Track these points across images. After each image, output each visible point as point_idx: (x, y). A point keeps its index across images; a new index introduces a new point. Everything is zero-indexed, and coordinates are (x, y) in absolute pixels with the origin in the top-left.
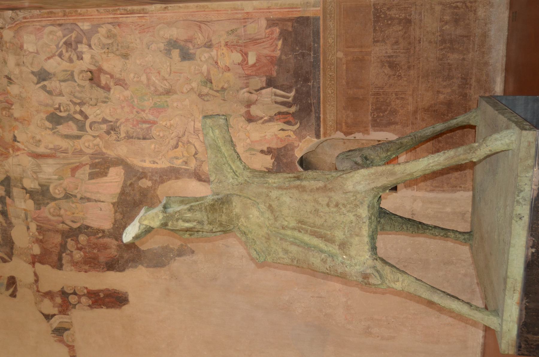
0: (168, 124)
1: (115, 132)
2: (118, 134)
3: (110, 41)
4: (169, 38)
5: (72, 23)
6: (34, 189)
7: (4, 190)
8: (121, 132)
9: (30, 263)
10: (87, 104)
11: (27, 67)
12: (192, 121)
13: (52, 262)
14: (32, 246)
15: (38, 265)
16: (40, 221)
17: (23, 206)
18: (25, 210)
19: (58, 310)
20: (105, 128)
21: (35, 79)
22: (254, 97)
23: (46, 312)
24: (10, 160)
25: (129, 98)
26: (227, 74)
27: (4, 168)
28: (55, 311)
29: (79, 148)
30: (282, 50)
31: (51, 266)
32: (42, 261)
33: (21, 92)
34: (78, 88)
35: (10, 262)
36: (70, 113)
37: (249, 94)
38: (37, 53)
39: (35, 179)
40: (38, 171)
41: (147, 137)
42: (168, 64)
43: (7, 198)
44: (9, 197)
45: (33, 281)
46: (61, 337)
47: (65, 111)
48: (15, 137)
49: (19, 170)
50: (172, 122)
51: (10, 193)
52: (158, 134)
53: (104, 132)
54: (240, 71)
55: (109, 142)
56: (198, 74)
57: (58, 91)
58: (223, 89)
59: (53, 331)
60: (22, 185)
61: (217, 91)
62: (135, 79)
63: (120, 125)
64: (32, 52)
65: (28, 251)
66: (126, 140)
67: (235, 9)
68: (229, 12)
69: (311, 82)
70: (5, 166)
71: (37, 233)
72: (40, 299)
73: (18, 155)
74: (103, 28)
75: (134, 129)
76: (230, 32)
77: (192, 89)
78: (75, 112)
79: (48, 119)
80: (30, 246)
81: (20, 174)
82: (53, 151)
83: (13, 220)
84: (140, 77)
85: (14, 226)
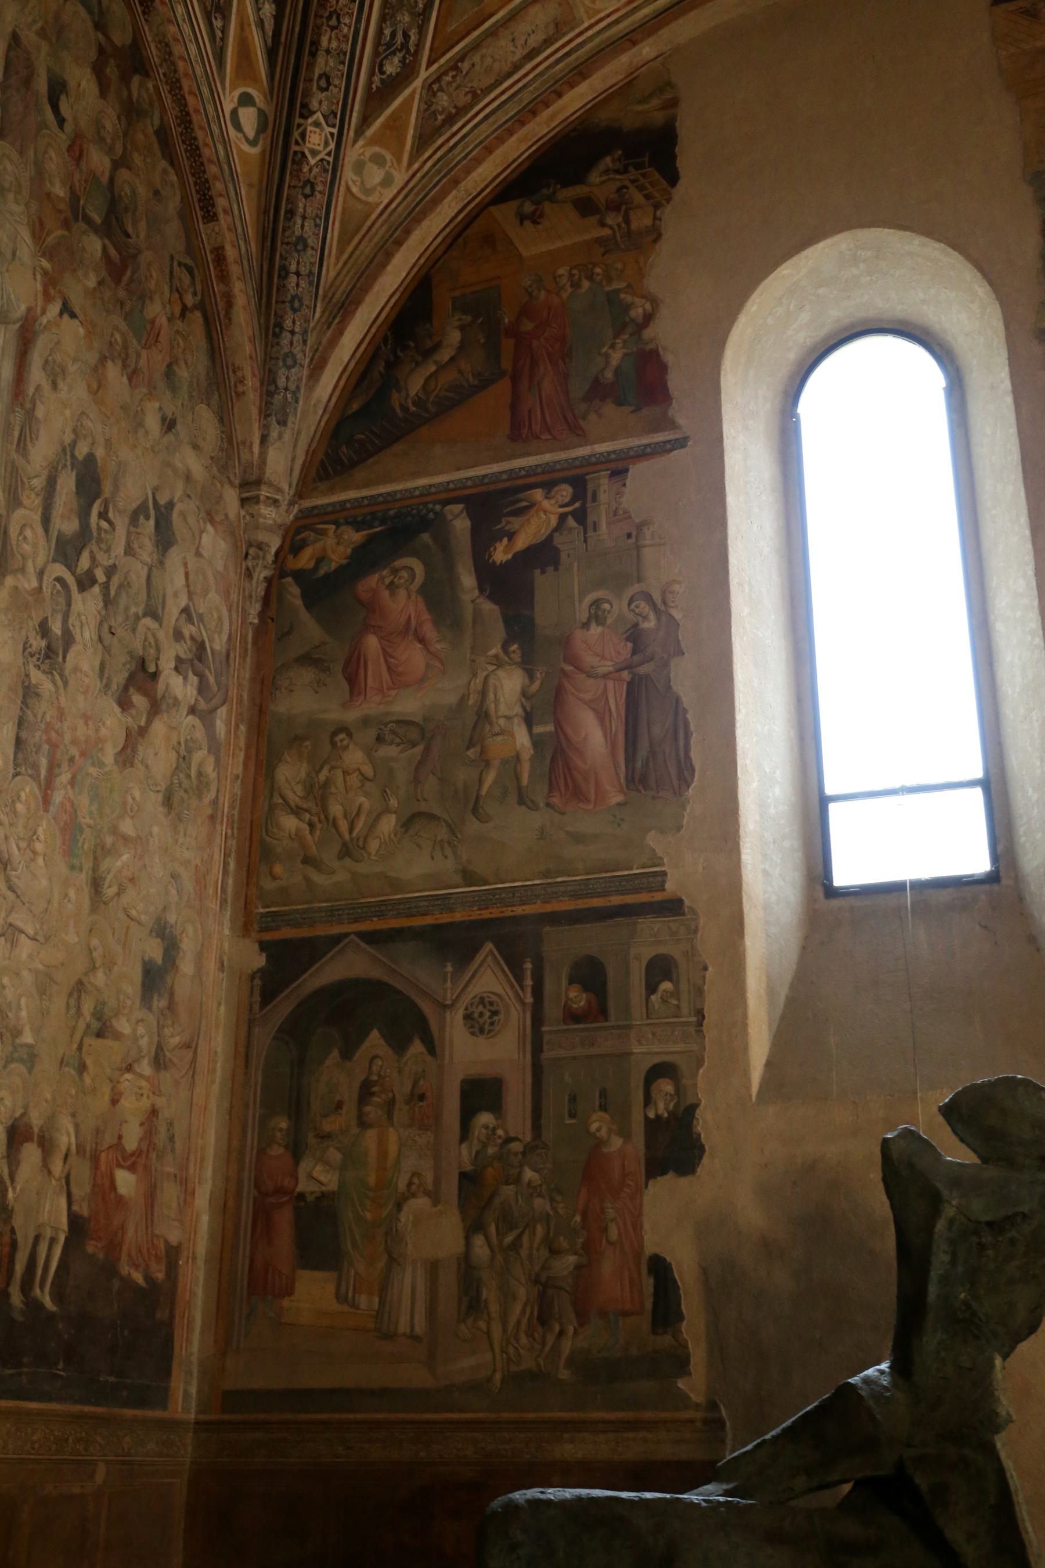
0: (39, 847)
1: (43, 652)
2: (39, 658)
3: (193, 773)
4: (181, 946)
5: (227, 690)
8: (43, 677)
10: (104, 612)
11: (181, 500)
12: (36, 934)
20: (53, 628)
21: (162, 501)
22: (57, 1167)
24: (25, 234)
25: (100, 755)
26: (106, 1090)
29: (26, 502)
30: (128, 1283)
34: (133, 610)
36: (93, 542)
37: (64, 1150)
38: (198, 554)
41: (20, 756)
42: (143, 918)
47: (99, 528)
48: (73, 316)
50: (40, 860)
52: (23, 795)
53: (47, 618)
54: (109, 1139)
55: (26, 616)
56: (118, 999)
57: (136, 546)
58: (82, 1068)
61: (80, 1048)
62: (129, 799)
63: (54, 683)
64: (200, 538)
66: (23, 674)
67: (203, 1160)
68: (200, 1141)
69: (63, 1370)
74: (214, 771)
75: (42, 721)
76: (171, 1131)
77: (94, 968)
78: (93, 558)
79: (90, 458)
82: (28, 406)
84: (132, 817)
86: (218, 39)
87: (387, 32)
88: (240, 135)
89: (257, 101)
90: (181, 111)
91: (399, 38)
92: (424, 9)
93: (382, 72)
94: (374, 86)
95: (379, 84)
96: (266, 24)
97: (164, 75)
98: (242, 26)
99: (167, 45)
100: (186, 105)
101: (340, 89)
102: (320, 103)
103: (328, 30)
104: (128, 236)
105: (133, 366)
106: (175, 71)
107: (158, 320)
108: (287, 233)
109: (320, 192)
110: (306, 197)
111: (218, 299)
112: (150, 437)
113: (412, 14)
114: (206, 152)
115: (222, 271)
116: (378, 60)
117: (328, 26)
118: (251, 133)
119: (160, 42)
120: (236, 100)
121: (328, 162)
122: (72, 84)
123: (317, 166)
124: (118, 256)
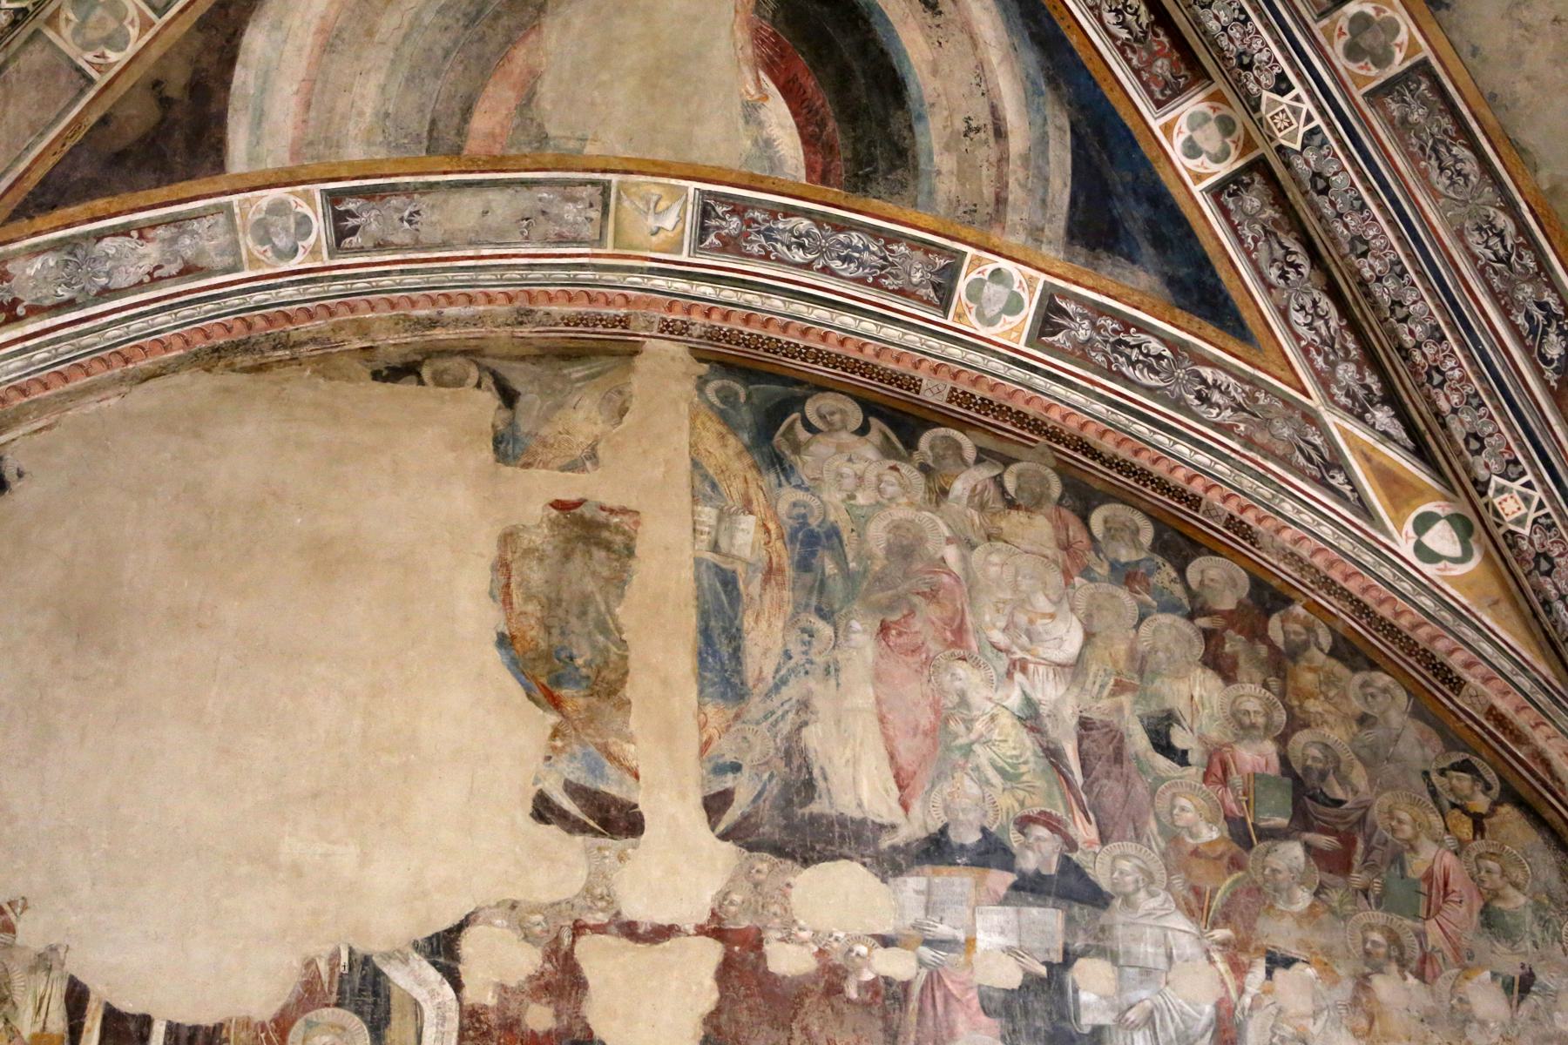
6: (1076, 1001)
7: (1044, 872)
9: (720, 920)
13: (737, 1022)
14: (803, 943)
15: (713, 952)
16: (929, 1001)
17: (984, 940)
18: (971, 942)
19: (486, 1007)
23: (468, 945)
24: (1179, 922)
27: (1138, 890)
28: (481, 990)
31: (718, 1011)
32: (733, 973)
33: (1483, 1024)
35: (713, 830)
39: (1122, 1013)
40: (1160, 1035)
43: (1011, 878)
44: (1015, 887)
45: (628, 914)
46: (334, 998)
48: (1288, 963)
49: (1148, 951)
51: (1032, 891)
59: (367, 960)
60: (1084, 953)
65: (777, 920)
70: (1152, 895)
71: (868, 976)
72: (538, 929)
73: (1211, 961)
80: (805, 935)
81: (1128, 953)
83: (913, 883)
85: (884, 881)
86: (1349, 494)
87: (1521, 320)
88: (1441, 565)
89: (1438, 511)
90: (1351, 603)
91: (1538, 315)
92: (1539, 264)
93: (1549, 362)
94: (1553, 383)
95: (1556, 377)
96: (1392, 431)
97: (1312, 582)
98: (1366, 457)
99: (1292, 554)
100: (1350, 595)
101: (1500, 431)
102: (1487, 466)
103: (1438, 390)
104: (1339, 803)
105: (1418, 954)
106: (1317, 571)
107: (1436, 867)
108: (1560, 628)
109: (1561, 555)
110: (1548, 573)
111: (1532, 765)
112: (1492, 1025)
113: (1529, 281)
114: (1404, 622)
115: (1511, 732)
116: (1536, 355)
117: (1435, 387)
118: (1455, 550)
119: (1285, 557)
120: (1412, 533)
121: (1547, 516)
122: (1180, 705)
123: (1533, 531)
124: (1332, 839)
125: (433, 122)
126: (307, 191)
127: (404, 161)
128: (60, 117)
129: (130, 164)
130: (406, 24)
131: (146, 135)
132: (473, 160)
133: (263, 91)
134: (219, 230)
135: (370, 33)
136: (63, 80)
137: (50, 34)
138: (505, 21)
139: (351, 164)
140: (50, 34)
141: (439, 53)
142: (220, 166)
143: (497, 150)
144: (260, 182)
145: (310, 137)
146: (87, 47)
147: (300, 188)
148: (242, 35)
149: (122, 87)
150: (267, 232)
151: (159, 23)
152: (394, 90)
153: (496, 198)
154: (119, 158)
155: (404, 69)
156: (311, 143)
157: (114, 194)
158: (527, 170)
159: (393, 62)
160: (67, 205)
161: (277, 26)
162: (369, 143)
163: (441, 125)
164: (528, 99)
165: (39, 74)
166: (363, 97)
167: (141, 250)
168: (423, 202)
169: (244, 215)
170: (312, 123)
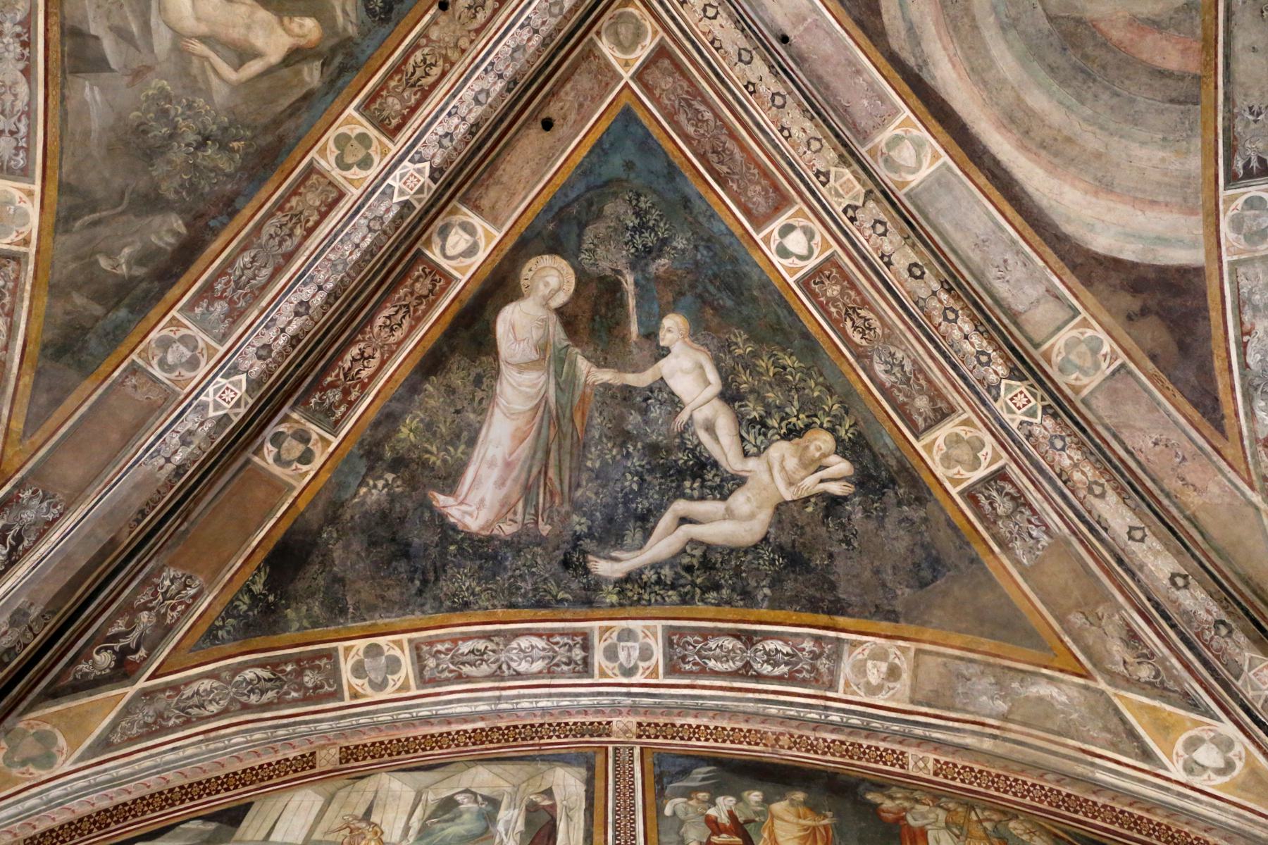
125: (1172, 101)
126: (1225, 201)
127: (1204, 123)
128: (1146, 390)
129: (1188, 340)
130: (1090, 128)
131: (1169, 327)
132: (1205, 65)
133: (1140, 237)
134: (1251, 272)
135: (1098, 156)
136: (1119, 385)
137: (1085, 392)
138: (1089, 50)
139: (1204, 167)
140: (1085, 392)
141: (1115, 101)
142: (1198, 271)
143: (1198, 46)
144: (1213, 240)
145: (1179, 200)
146: (1097, 367)
147: (1221, 207)
148: (1097, 253)
149: (1129, 342)
150: (1256, 233)
151: (1084, 314)
152: (1144, 135)
153: (1239, 44)
154: (1183, 348)
155: (1127, 128)
156: (1185, 199)
157: (1211, 353)
158: (1216, 18)
159: (1121, 137)
160: (1216, 389)
161: (1091, 228)
162: (1188, 152)
163: (1174, 94)
164: (1155, 24)
165: (1113, 402)
166: (1149, 160)
167: (1261, 333)
168: (1241, 103)
169: (1241, 252)
170: (1168, 199)
